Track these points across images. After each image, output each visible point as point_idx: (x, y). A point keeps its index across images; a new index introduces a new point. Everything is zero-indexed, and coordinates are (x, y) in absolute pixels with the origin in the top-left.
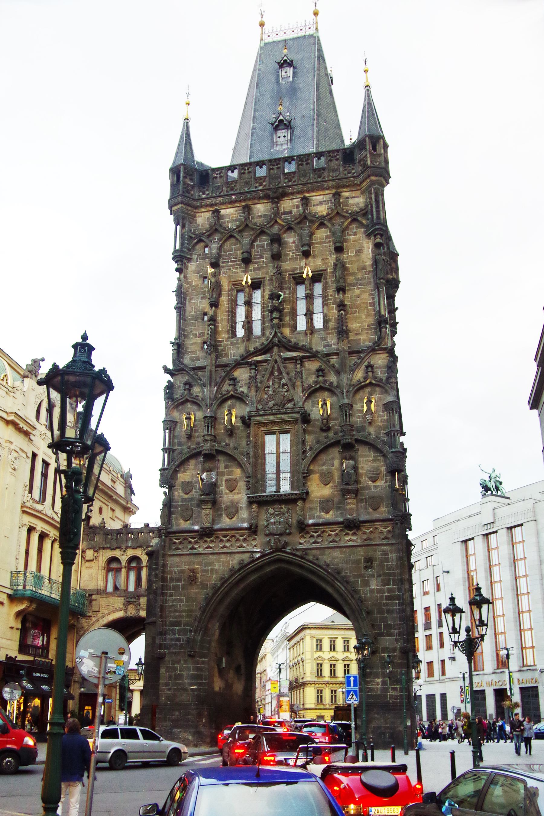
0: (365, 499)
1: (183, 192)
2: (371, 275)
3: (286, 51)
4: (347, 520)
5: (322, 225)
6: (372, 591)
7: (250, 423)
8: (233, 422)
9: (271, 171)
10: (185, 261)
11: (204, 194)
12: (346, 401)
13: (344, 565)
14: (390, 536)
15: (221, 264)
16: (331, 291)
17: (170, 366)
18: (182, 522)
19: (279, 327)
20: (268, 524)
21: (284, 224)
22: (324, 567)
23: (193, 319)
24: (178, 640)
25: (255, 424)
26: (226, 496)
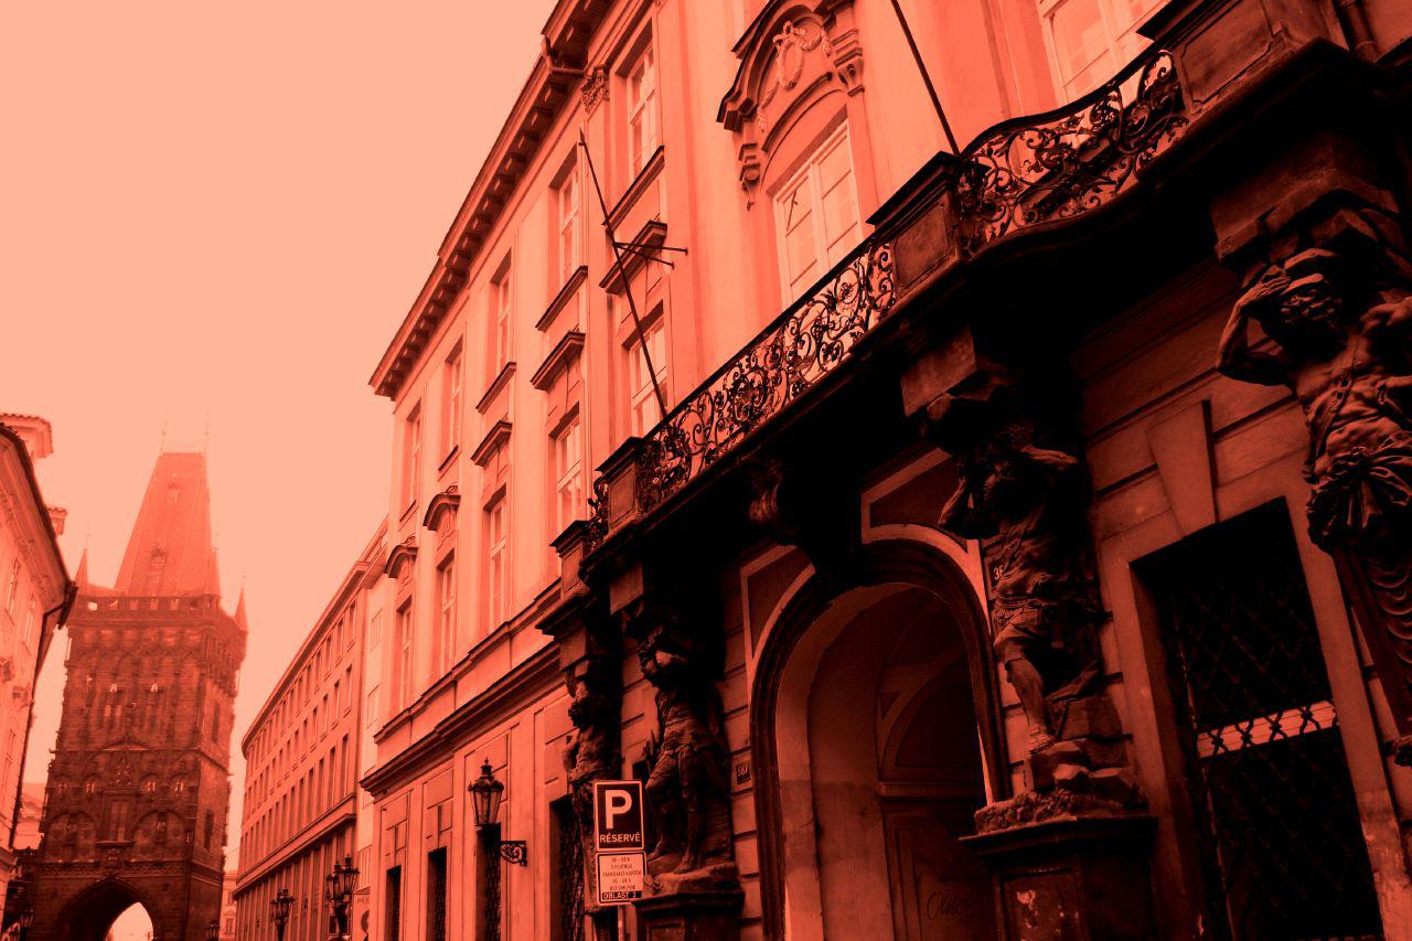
5: (169, 654)
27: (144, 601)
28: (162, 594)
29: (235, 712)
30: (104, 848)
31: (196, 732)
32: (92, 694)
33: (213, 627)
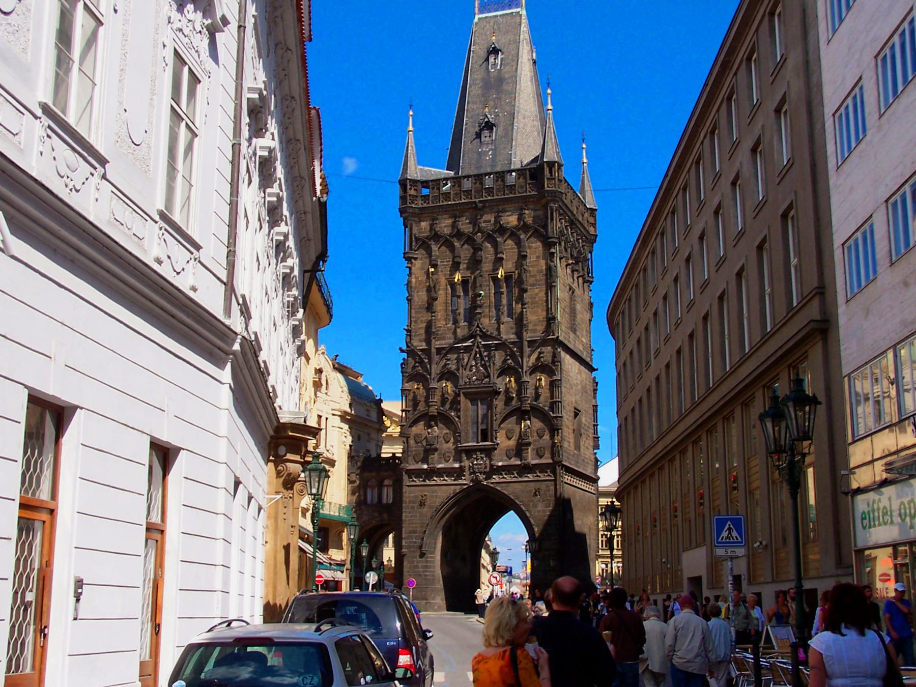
3: (494, 38)
6: (538, 511)
10: (413, 261)
15: (439, 263)
17: (404, 348)
24: (415, 542)
28: (498, 169)
30: (469, 452)
31: (550, 320)
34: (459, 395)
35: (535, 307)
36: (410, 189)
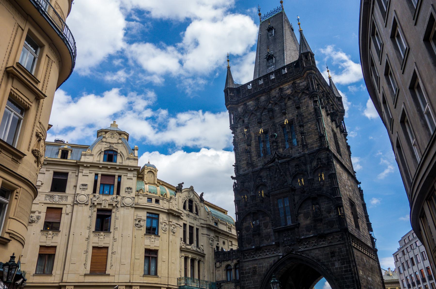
0: (326, 222)
1: (230, 99)
2: (314, 116)
4: (319, 234)
5: (289, 99)
6: (337, 268)
7: (270, 196)
8: (263, 196)
9: (265, 80)
11: (239, 98)
12: (310, 178)
13: (321, 257)
14: (341, 239)
15: (250, 127)
16: (298, 128)
17: (234, 176)
18: (247, 245)
19: (277, 149)
20: (284, 241)
21: (273, 102)
22: (312, 259)
23: (242, 153)
25: (272, 195)
26: (264, 231)
27: (266, 77)
29: (349, 145)
31: (322, 137)
32: (249, 136)
33: (313, 71)
34: (269, 197)
35: (310, 134)
36: (230, 93)
